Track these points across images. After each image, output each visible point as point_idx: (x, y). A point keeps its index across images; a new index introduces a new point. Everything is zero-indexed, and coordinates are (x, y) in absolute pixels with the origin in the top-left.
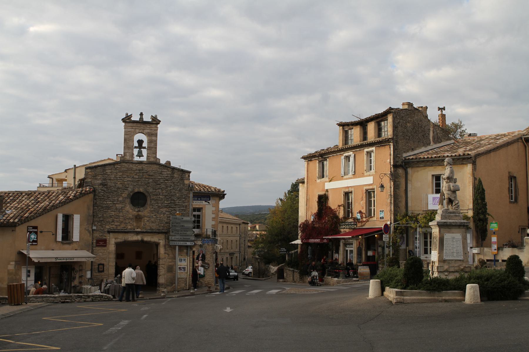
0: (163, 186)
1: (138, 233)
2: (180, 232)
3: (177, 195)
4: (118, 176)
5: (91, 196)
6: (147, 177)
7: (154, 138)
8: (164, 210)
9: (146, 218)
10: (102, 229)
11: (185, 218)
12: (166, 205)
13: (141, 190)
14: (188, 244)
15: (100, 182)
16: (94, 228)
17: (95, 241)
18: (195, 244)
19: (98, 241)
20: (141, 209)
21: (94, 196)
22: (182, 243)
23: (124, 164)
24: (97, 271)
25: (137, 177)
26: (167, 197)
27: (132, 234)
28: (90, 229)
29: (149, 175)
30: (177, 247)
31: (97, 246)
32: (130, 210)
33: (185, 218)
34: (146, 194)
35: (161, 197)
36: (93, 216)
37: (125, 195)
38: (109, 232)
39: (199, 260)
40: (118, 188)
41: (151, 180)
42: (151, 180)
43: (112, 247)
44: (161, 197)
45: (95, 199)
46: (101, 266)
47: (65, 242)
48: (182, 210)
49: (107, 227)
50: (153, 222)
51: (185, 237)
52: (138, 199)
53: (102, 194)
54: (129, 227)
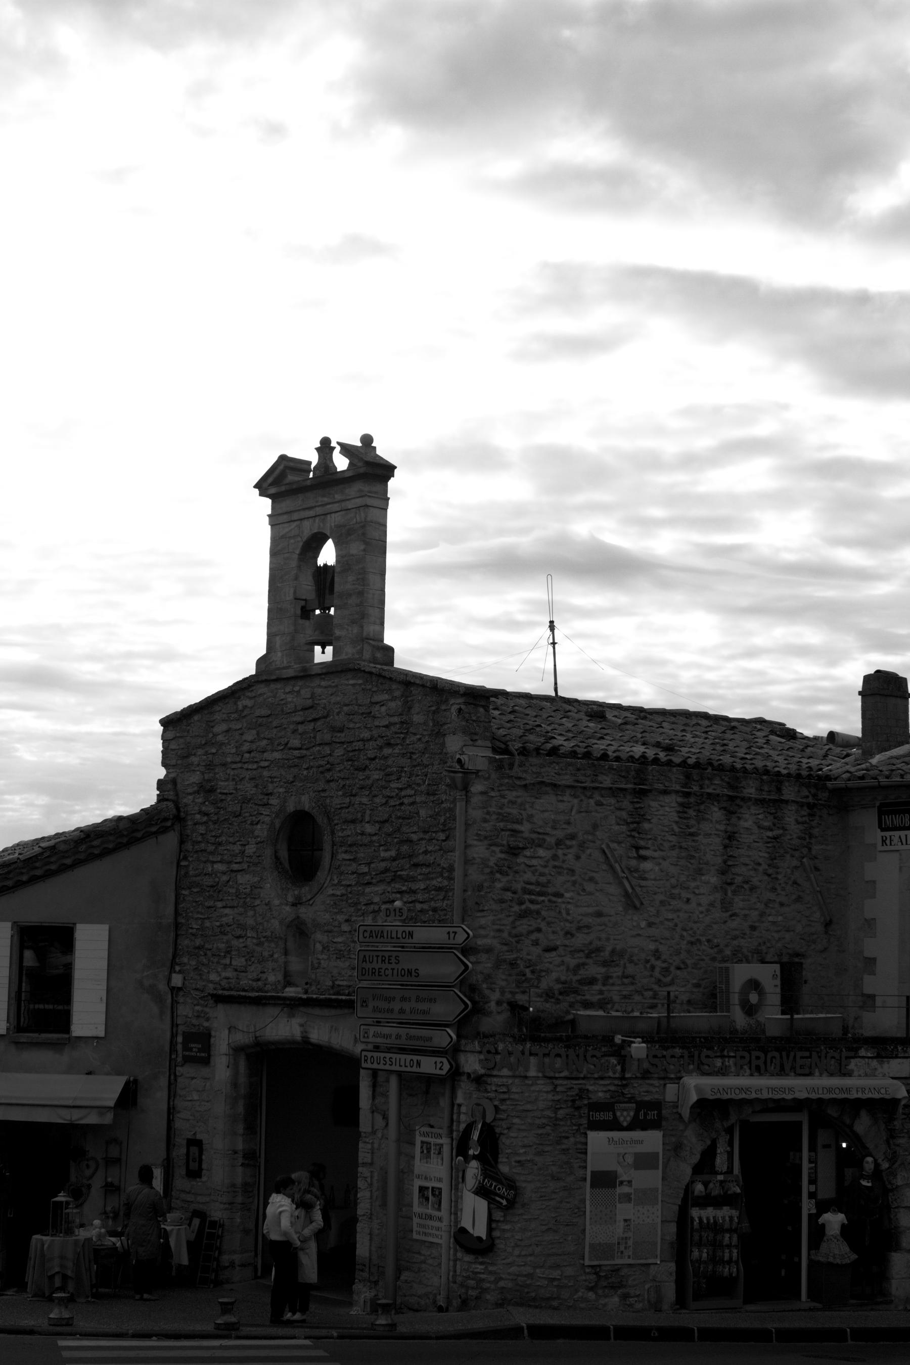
0: (376, 775)
1: (293, 1005)
2: (396, 1005)
3: (423, 813)
4: (246, 747)
5: (170, 840)
6: (327, 737)
7: (356, 548)
8: (375, 893)
9: (319, 936)
10: (200, 985)
11: (423, 934)
12: (383, 865)
13: (306, 802)
14: (429, 1065)
15: (195, 778)
16: (177, 980)
17: (180, 1039)
18: (456, 1073)
19: (189, 1038)
20: (305, 891)
21: (182, 842)
22: (403, 1062)
23: (262, 689)
24: (184, 1172)
25: (295, 742)
26: (388, 828)
27: (272, 1011)
28: (162, 987)
29: (334, 729)
30: (394, 1082)
31: (187, 1060)
32: (274, 896)
33: (423, 934)
34: (321, 820)
35: (369, 829)
36: (177, 926)
37: (261, 831)
38: (219, 999)
39: (467, 1159)
40: (246, 801)
41: (339, 752)
42: (339, 752)
43: (222, 1069)
44: (369, 829)
45: (182, 856)
46: (194, 1150)
47: (24, 1037)
48: (439, 889)
49: (213, 977)
50: (340, 955)
51: (413, 1032)
52: (301, 848)
53: (202, 829)
54: (272, 978)
